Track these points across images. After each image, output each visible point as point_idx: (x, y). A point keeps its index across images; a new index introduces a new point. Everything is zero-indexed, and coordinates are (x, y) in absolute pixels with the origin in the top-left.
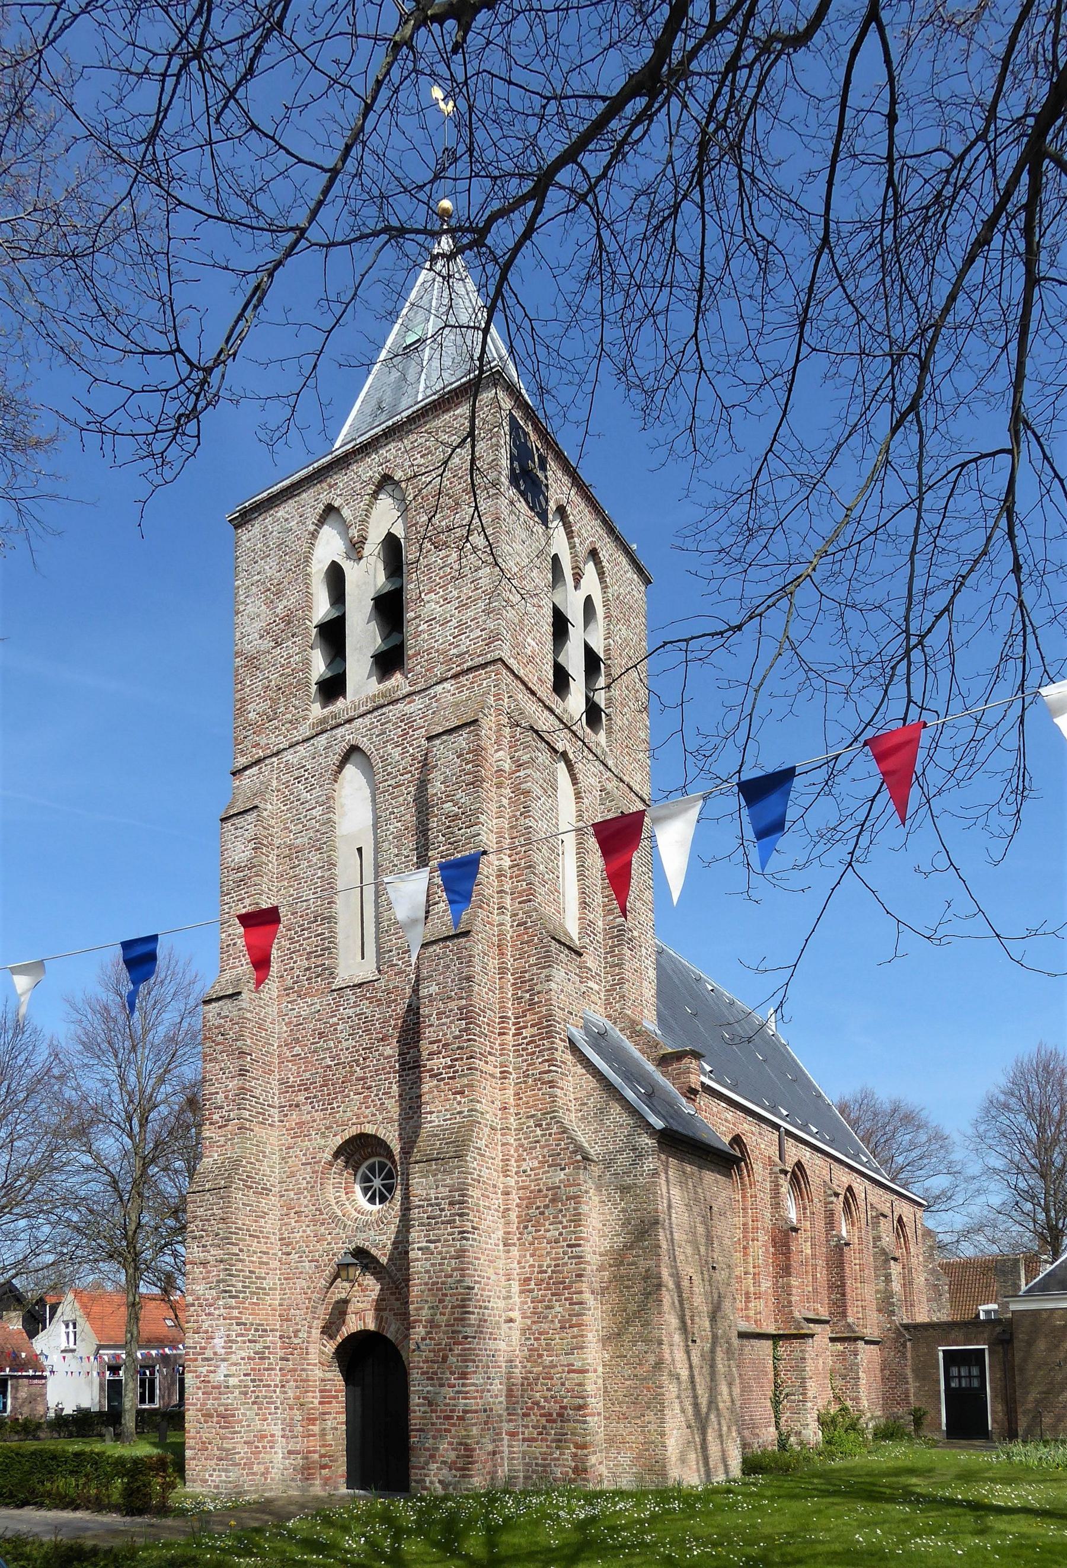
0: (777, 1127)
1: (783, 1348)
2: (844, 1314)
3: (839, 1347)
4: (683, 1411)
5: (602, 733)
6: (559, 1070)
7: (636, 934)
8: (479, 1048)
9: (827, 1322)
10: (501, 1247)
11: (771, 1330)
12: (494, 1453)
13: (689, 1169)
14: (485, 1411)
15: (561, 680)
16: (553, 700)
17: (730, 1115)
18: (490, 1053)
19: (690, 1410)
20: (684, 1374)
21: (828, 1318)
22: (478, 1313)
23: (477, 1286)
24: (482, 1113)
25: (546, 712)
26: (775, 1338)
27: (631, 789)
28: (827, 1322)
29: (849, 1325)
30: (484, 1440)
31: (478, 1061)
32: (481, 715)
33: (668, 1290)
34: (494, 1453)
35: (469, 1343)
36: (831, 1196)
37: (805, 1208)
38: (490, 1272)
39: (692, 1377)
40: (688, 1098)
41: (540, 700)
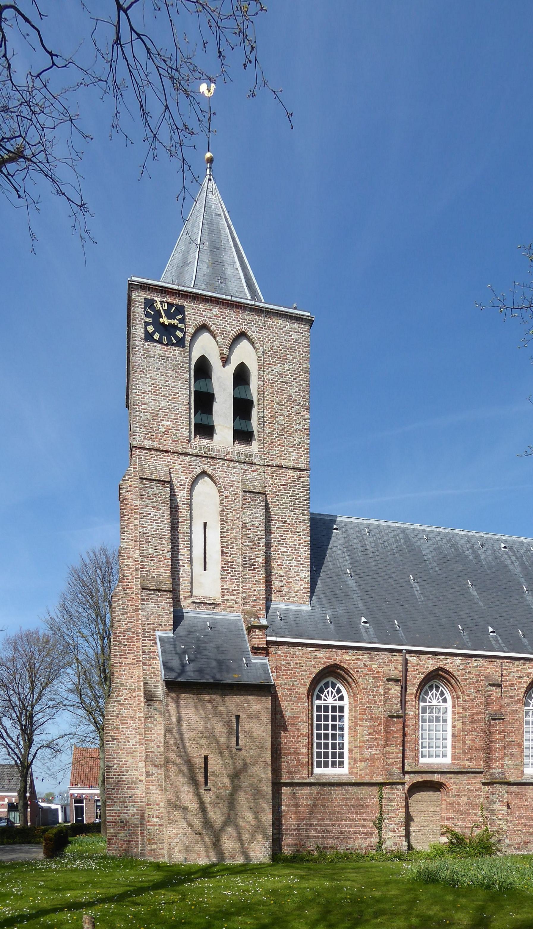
0: (400, 651)
1: (386, 790)
2: (489, 767)
3: (486, 789)
4: (190, 825)
5: (255, 443)
6: (148, 656)
7: (258, 559)
8: (119, 652)
9: (481, 772)
10: (138, 746)
11: (380, 780)
12: (130, 841)
13: (207, 697)
14: (123, 822)
15: (205, 430)
16: (200, 443)
17: (322, 653)
18: (128, 653)
19: (198, 824)
20: (193, 806)
21: (482, 770)
22: (116, 778)
23: (115, 766)
24: (122, 684)
25: (182, 457)
26: (381, 785)
27: (281, 467)
28: (481, 772)
29: (492, 774)
30: (120, 835)
31: (118, 659)
32: (122, 482)
33: (174, 763)
34: (130, 841)
35: (109, 791)
36: (487, 686)
37: (458, 698)
38: (129, 759)
39: (203, 809)
40: (255, 653)
41: (174, 453)
